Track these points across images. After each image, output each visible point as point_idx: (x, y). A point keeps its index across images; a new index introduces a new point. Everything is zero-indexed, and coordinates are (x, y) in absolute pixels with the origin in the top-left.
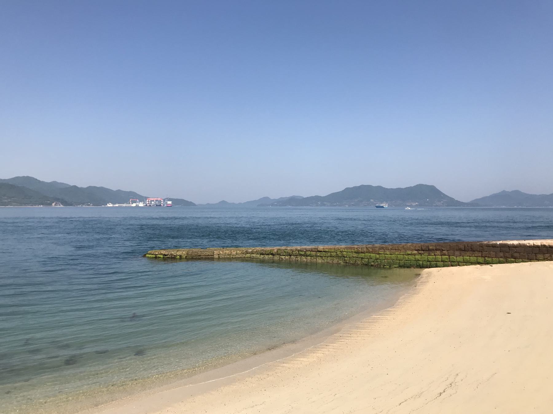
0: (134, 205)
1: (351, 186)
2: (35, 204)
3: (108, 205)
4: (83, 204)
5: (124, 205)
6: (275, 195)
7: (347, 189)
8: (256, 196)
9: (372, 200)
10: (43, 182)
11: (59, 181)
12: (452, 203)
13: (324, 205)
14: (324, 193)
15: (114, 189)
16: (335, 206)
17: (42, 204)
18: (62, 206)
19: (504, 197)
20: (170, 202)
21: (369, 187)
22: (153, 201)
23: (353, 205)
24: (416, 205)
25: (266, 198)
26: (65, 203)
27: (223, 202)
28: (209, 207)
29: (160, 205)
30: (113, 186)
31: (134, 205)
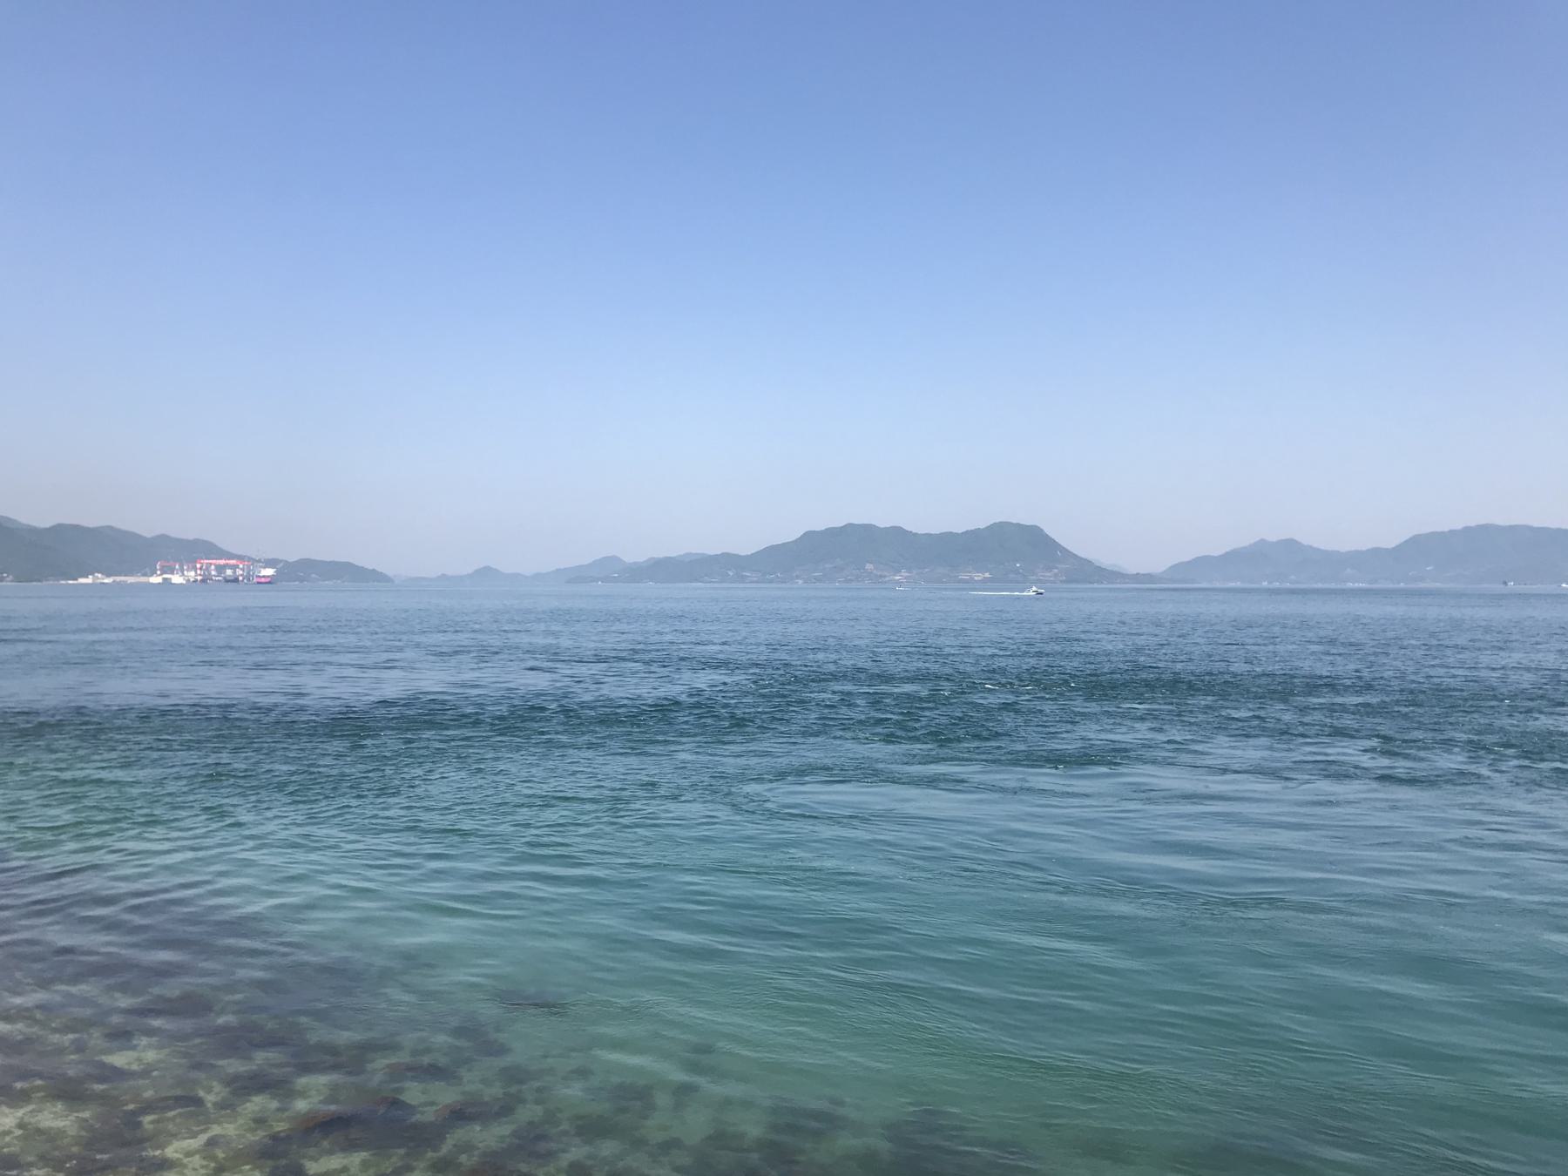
0: (156, 580)
1: (820, 526)
3: (89, 580)
5: (130, 580)
6: (635, 554)
7: (809, 535)
8: (582, 555)
9: (869, 566)
12: (1086, 572)
13: (742, 579)
14: (747, 544)
16: (771, 581)
19: (1257, 555)
20: (269, 572)
21: (868, 529)
23: (818, 580)
24: (985, 580)
25: (614, 559)
29: (236, 580)
30: (146, 525)
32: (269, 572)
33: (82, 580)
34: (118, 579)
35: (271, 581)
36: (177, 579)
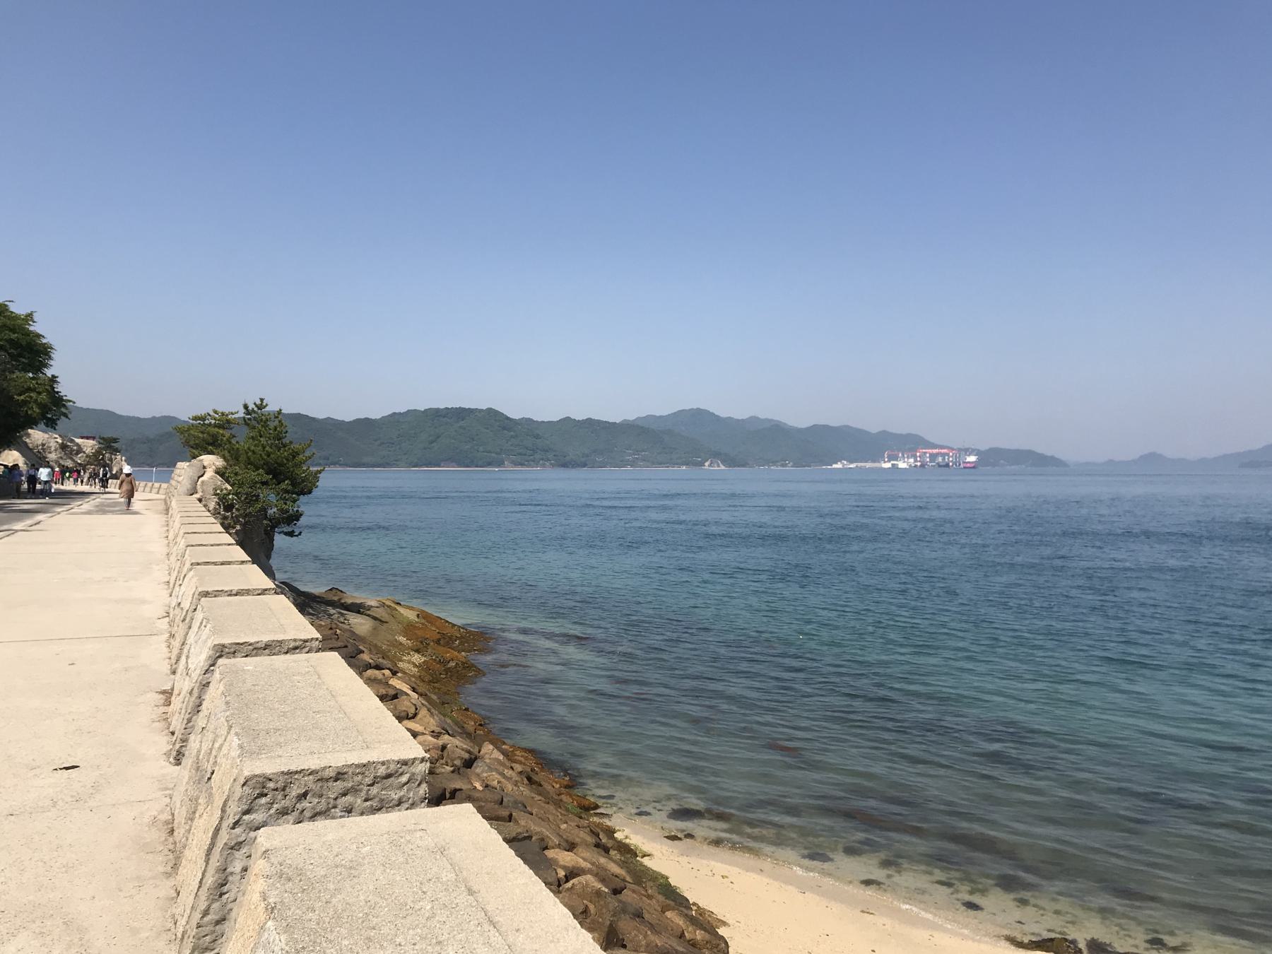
0: (888, 465)
2: (674, 464)
3: (839, 466)
4: (774, 463)
5: (868, 465)
10: (395, 418)
11: (762, 416)
15: (874, 429)
17: (687, 464)
18: (723, 467)
20: (972, 459)
22: (938, 454)
26: (731, 462)
27: (1151, 458)
28: (1111, 469)
29: (947, 465)
31: (888, 465)
32: (972, 459)
33: (835, 466)
34: (860, 464)
35: (974, 466)
36: (902, 465)
